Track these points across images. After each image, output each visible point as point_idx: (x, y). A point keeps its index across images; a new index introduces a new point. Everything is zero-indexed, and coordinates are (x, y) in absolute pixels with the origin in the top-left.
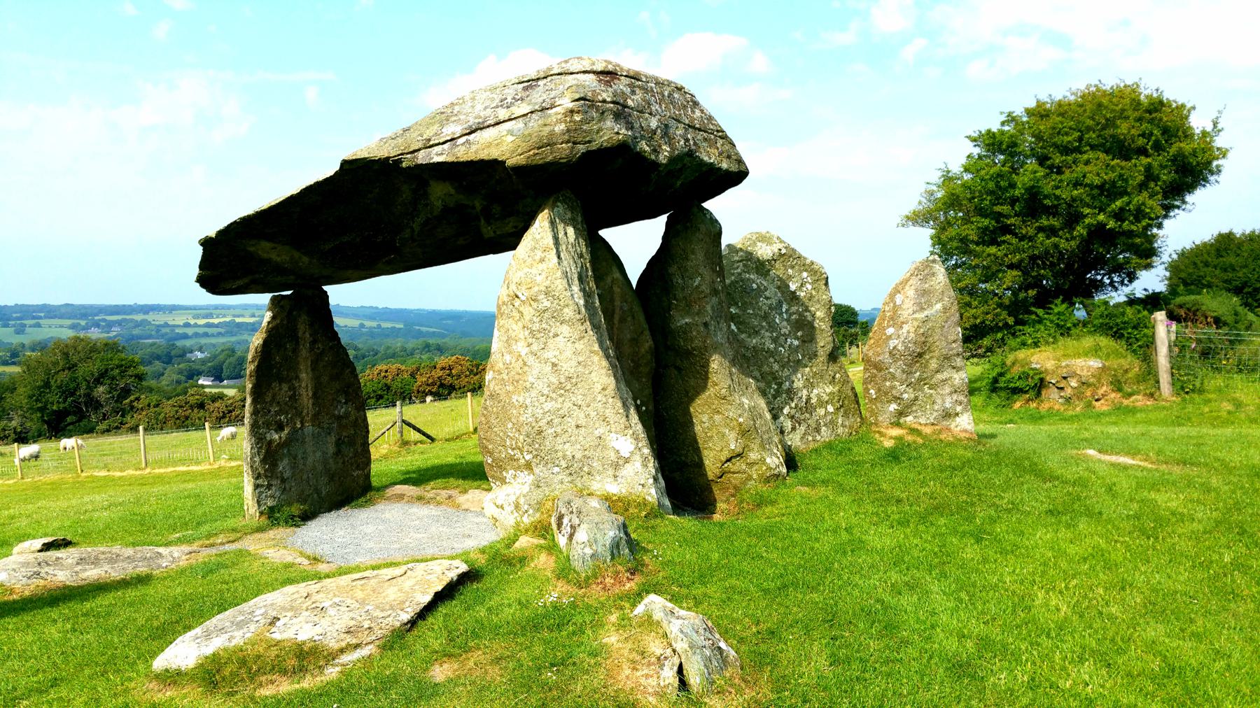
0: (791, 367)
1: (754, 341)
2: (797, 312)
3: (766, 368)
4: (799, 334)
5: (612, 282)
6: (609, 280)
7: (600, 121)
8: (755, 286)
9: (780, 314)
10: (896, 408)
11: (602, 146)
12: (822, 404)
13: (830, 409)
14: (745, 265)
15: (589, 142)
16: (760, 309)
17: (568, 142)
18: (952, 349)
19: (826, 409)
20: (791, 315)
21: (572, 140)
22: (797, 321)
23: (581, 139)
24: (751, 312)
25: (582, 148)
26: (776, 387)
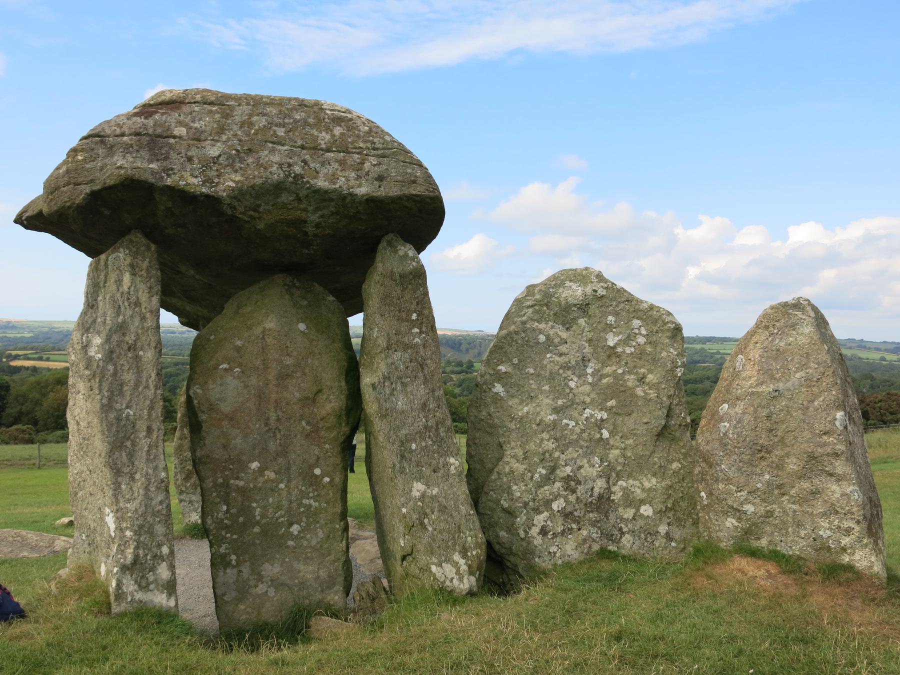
0: (581, 447)
1: (526, 409)
2: (614, 375)
3: (532, 446)
4: (612, 403)
5: (263, 332)
6: (258, 331)
7: (106, 157)
8: (542, 338)
9: (582, 375)
10: (736, 524)
11: (105, 183)
12: (630, 501)
13: (646, 510)
14: (536, 312)
15: (92, 181)
16: (543, 367)
17: (68, 184)
18: (825, 444)
19: (638, 510)
20: (603, 377)
21: (72, 181)
22: (609, 386)
23: (83, 179)
24: (532, 371)
25: (87, 189)
26: (544, 472)
